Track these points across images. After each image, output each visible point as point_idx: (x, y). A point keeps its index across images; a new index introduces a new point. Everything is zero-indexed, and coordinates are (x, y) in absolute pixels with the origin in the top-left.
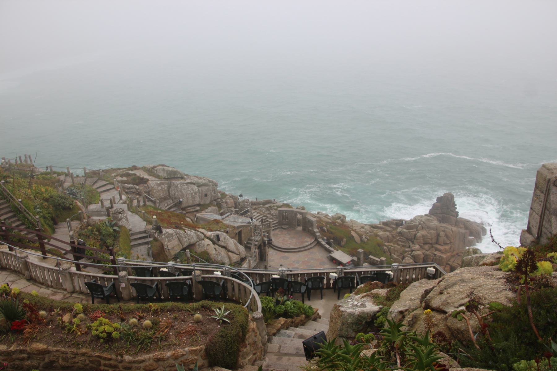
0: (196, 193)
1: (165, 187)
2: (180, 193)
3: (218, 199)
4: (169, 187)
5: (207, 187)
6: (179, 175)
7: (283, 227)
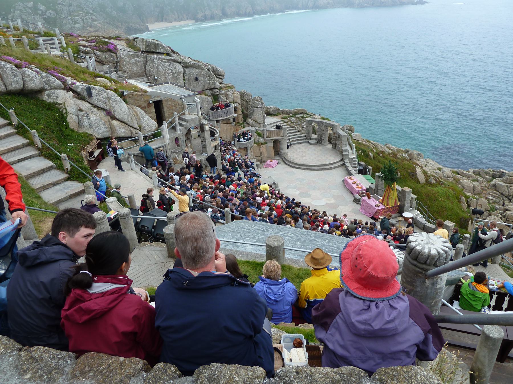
0: (179, 74)
1: (140, 60)
2: (156, 70)
3: (215, 88)
4: (146, 62)
5: (198, 70)
6: (162, 51)
7: (310, 141)
